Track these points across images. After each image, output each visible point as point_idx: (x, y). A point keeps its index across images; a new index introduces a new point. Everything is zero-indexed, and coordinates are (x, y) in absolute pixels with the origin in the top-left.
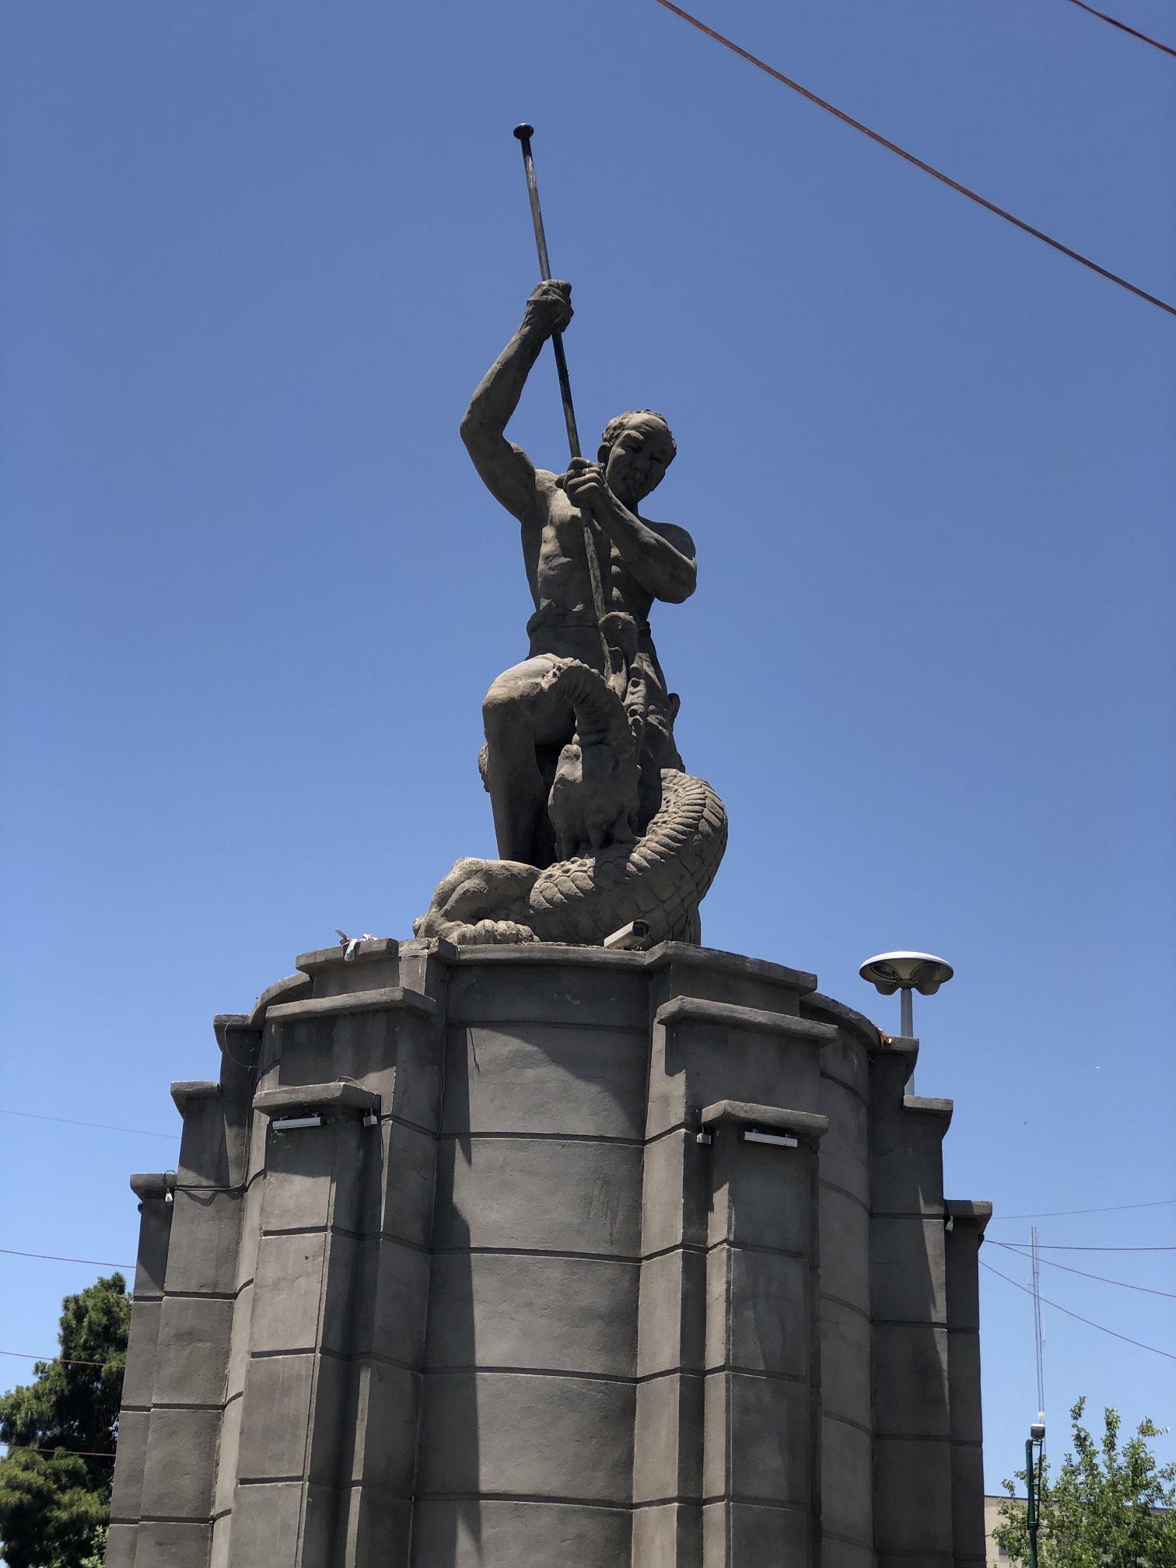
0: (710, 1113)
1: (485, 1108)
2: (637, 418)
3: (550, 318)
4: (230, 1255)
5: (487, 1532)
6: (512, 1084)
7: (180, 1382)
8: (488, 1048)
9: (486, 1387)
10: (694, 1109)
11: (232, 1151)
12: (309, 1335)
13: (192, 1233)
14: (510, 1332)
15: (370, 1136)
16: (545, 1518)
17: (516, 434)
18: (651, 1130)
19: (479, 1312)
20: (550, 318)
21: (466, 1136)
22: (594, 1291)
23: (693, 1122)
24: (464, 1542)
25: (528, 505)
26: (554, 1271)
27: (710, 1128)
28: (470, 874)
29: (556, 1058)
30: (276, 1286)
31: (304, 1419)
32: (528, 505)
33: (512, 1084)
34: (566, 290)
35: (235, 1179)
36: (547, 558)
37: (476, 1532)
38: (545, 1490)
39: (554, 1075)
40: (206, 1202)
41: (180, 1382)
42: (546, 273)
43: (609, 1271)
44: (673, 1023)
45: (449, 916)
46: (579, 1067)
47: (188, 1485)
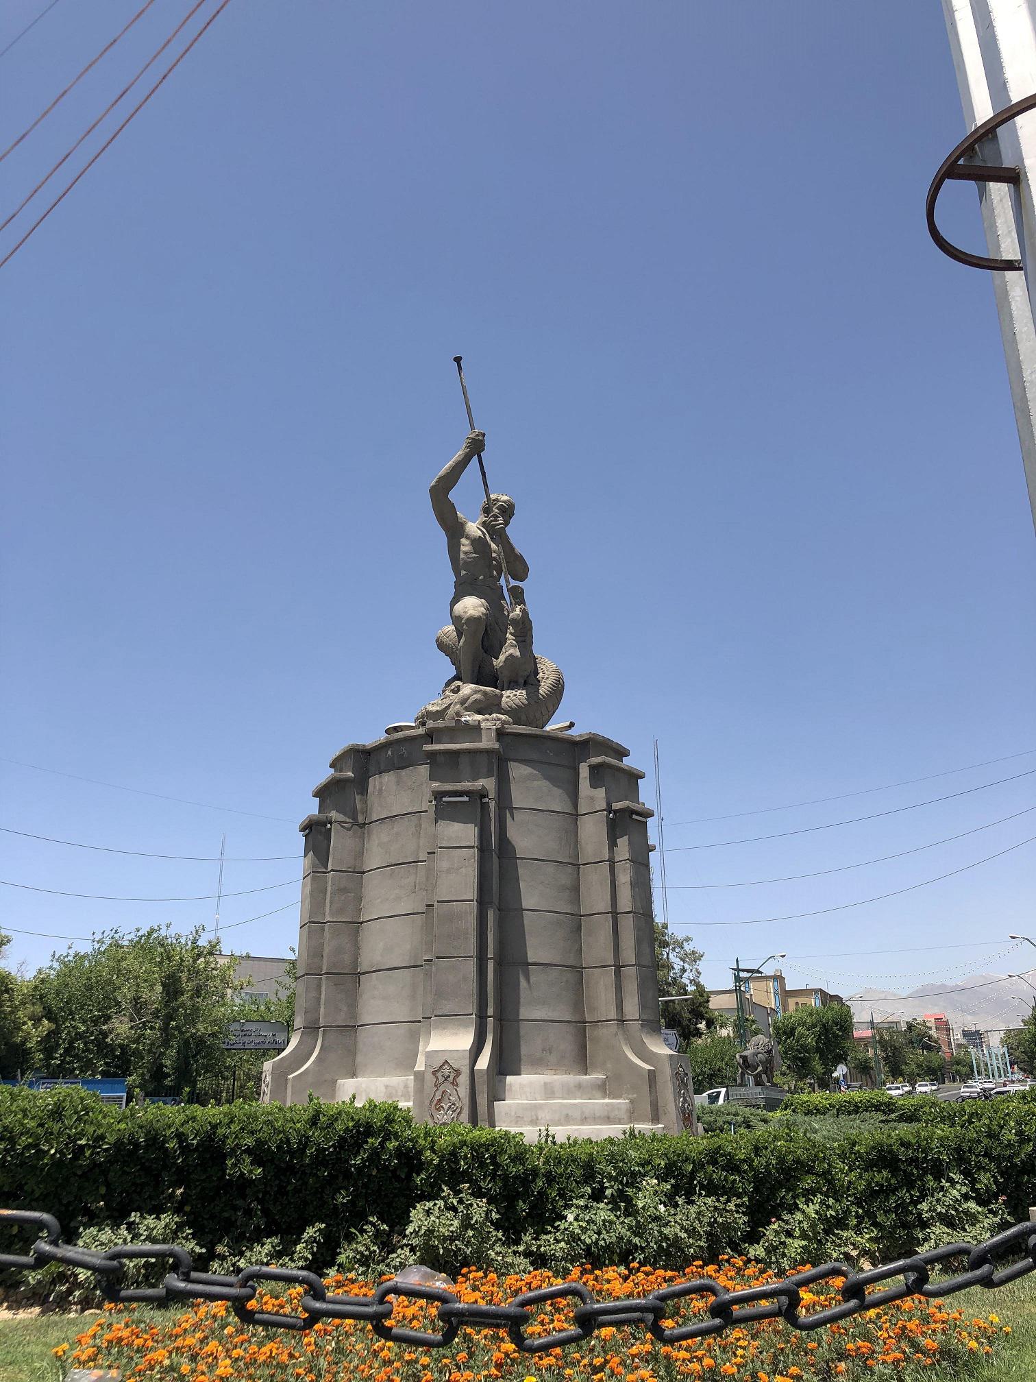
0: (617, 805)
1: (518, 797)
2: (505, 498)
3: (476, 447)
4: (360, 854)
5: (532, 979)
6: (529, 787)
7: (341, 911)
8: (518, 771)
9: (528, 918)
10: (609, 805)
11: (359, 806)
12: (471, 893)
13: (340, 843)
14: (536, 894)
15: (485, 807)
16: (554, 973)
17: (453, 496)
18: (581, 810)
19: (522, 885)
20: (476, 447)
21: (512, 809)
22: (565, 879)
23: (609, 809)
24: (523, 983)
25: (454, 529)
26: (550, 869)
27: (615, 812)
28: (476, 692)
29: (547, 778)
30: (448, 871)
31: (471, 931)
32: (454, 529)
33: (529, 787)
34: (484, 435)
35: (361, 820)
36: (466, 553)
37: (528, 981)
38: (554, 962)
39: (544, 784)
40: (349, 829)
41: (341, 911)
42: (472, 428)
43: (569, 869)
44: (593, 768)
45: (467, 709)
46: (555, 782)
47: (347, 958)
